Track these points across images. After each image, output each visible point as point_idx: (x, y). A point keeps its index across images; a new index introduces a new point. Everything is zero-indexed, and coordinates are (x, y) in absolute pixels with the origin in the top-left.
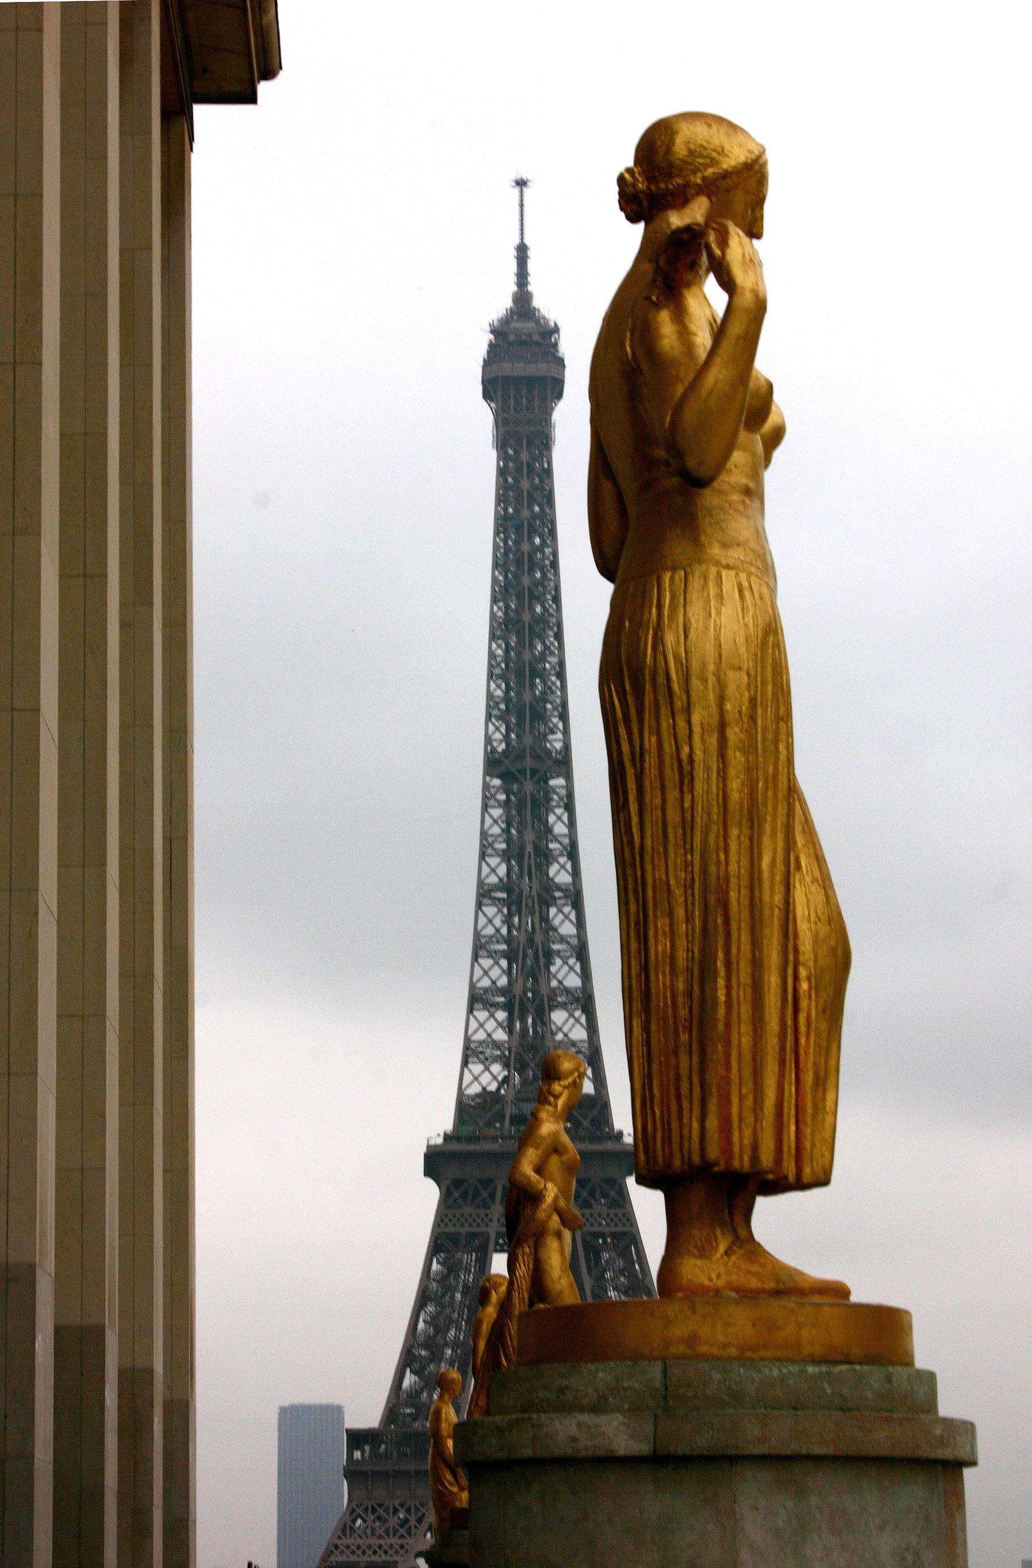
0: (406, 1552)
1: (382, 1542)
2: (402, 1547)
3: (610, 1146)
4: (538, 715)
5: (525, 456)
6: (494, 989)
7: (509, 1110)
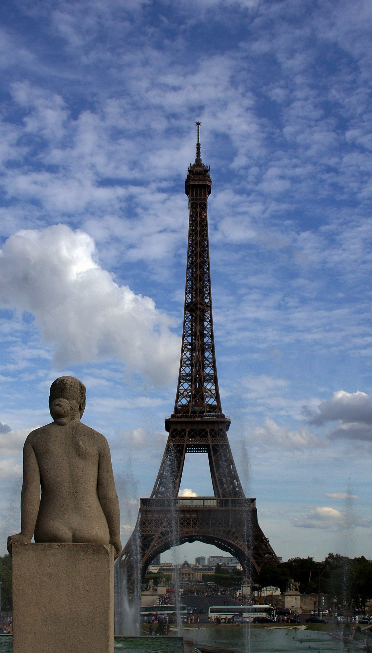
2: (156, 531)
3: (222, 419)
4: (202, 293)
6: (187, 375)
7: (191, 409)
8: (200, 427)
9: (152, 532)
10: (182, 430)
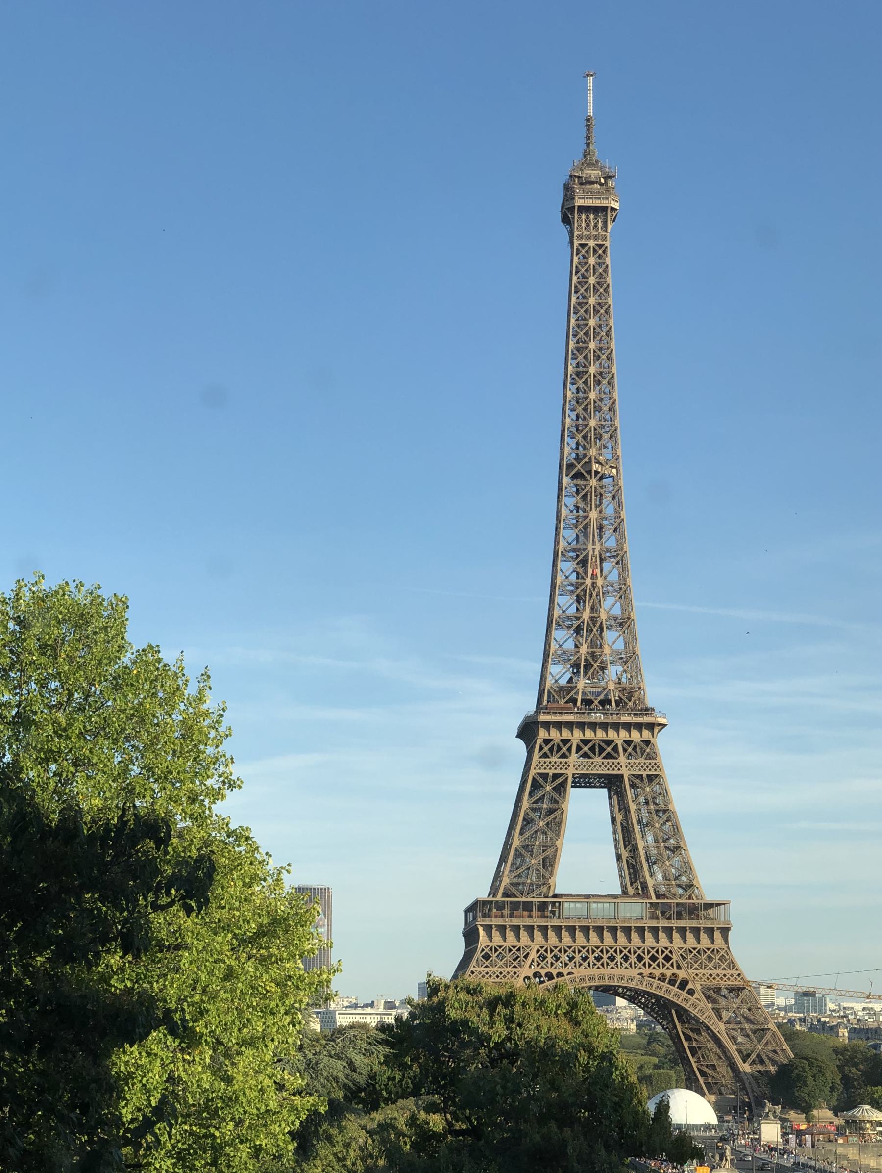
2: (515, 973)
5: (592, 261)
8: (601, 734)
9: (505, 976)
10: (562, 740)
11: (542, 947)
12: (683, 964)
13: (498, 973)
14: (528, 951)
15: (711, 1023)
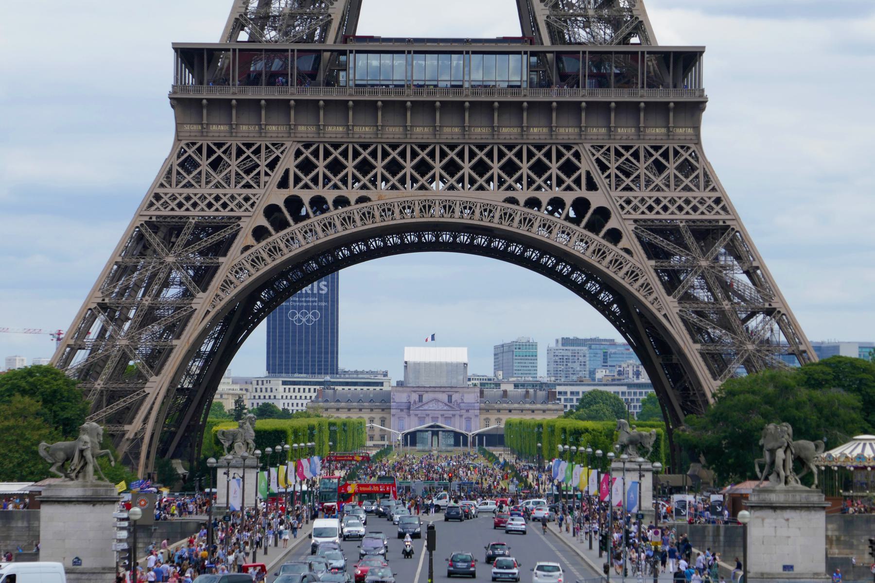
0: (252, 205)
1: (220, 191)
2: (247, 199)
9: (225, 206)
11: (307, 146)
12: (599, 178)
13: (210, 199)
14: (278, 153)
15: (651, 298)
